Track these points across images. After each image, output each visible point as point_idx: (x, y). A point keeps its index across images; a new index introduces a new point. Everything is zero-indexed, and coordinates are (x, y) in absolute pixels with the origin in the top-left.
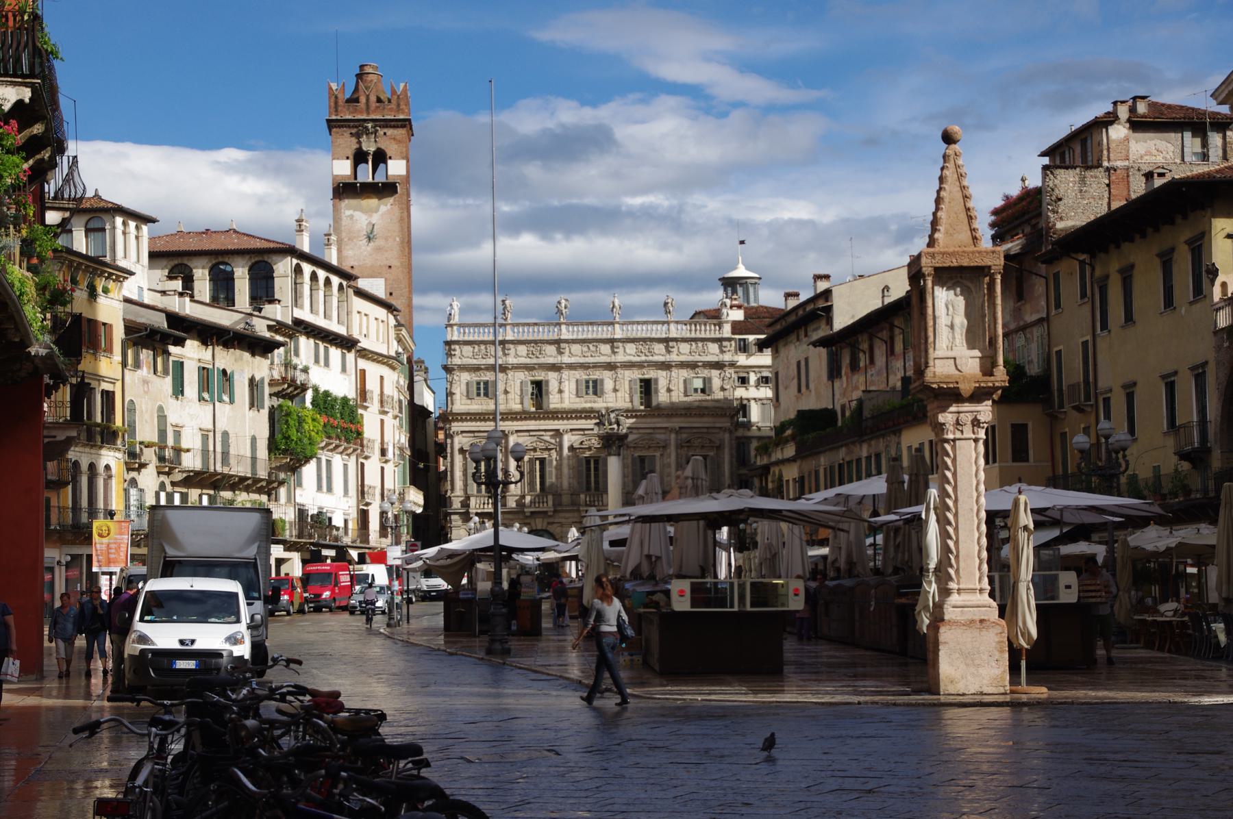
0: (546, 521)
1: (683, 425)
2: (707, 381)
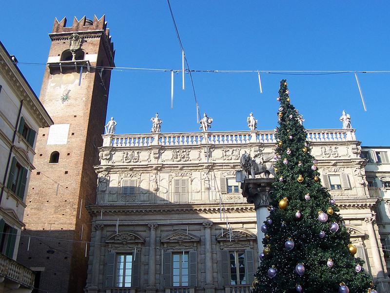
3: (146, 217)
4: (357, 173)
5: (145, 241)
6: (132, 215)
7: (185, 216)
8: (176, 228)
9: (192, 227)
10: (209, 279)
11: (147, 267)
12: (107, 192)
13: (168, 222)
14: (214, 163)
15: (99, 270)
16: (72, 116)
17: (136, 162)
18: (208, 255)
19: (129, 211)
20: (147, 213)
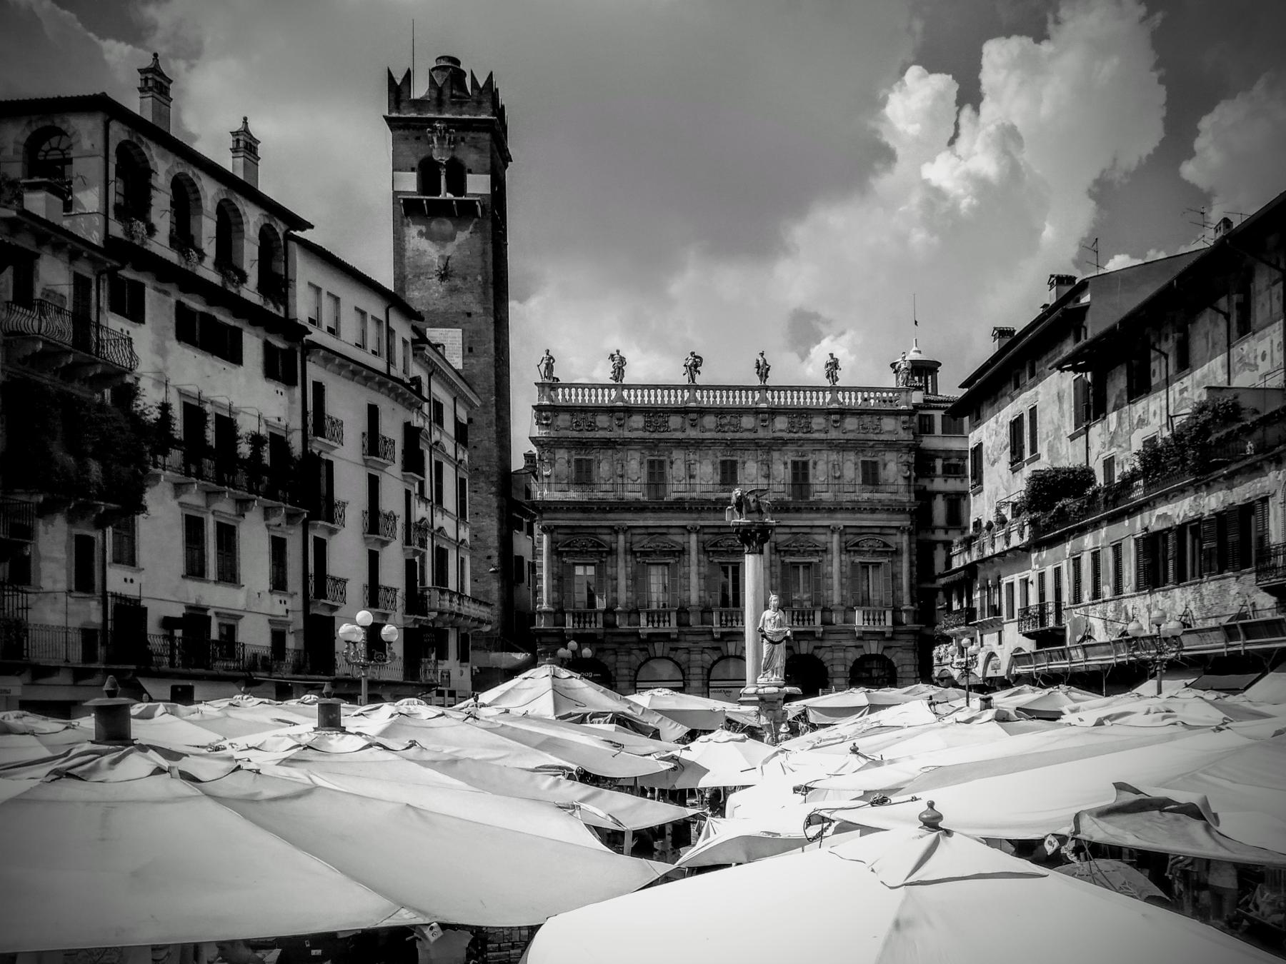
0: (669, 645)
1: (848, 523)
9: (672, 531)
13: (641, 523)
16: (464, 313)
18: (694, 569)
20: (611, 511)
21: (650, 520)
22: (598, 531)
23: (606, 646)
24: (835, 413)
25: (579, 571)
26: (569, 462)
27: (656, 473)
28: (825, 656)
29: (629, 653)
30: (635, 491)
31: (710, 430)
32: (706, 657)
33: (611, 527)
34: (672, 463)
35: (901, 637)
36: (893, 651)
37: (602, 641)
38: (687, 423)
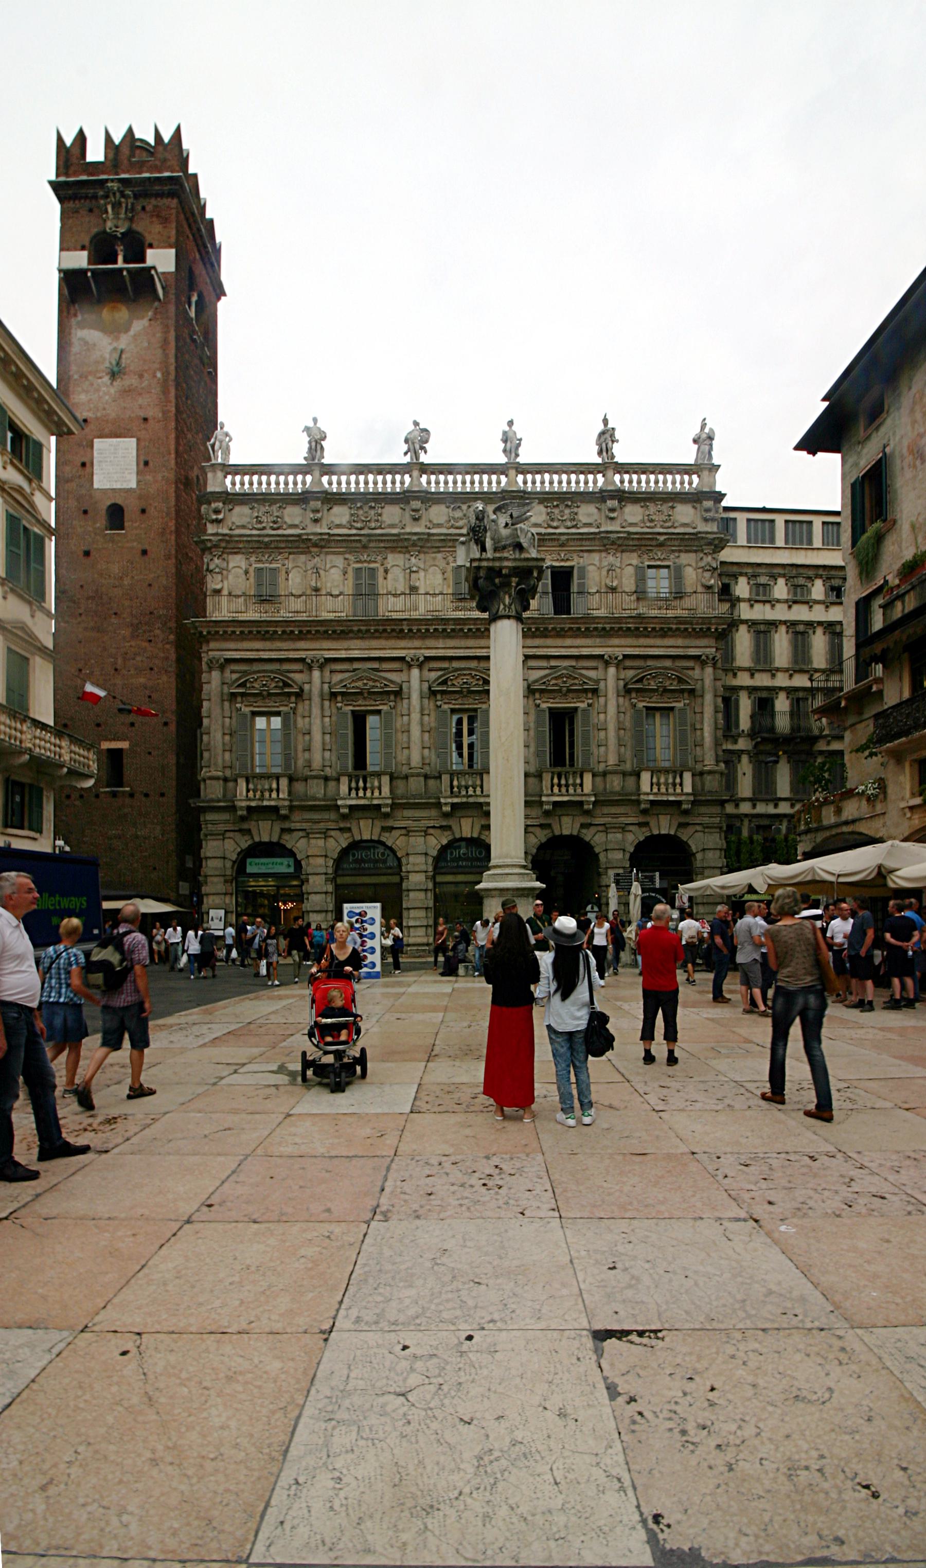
0: (378, 824)
2: (677, 575)
3: (302, 644)
4: (702, 564)
5: (302, 690)
6: (274, 639)
7: (374, 643)
8: (356, 665)
9: (386, 666)
10: (416, 760)
11: (307, 737)
12: (225, 592)
13: (343, 654)
14: (429, 534)
15: (224, 744)
17: (278, 529)
18: (415, 716)
19: (267, 632)
20: (302, 636)
21: (355, 649)
22: (286, 667)
23: (293, 826)
24: (612, 498)
25: (261, 723)
26: (246, 572)
27: (366, 591)
28: (596, 839)
29: (325, 834)
30: (332, 609)
31: (439, 526)
32: (432, 841)
33: (302, 660)
34: (386, 571)
35: (703, 809)
36: (691, 830)
37: (285, 818)
38: (408, 514)
